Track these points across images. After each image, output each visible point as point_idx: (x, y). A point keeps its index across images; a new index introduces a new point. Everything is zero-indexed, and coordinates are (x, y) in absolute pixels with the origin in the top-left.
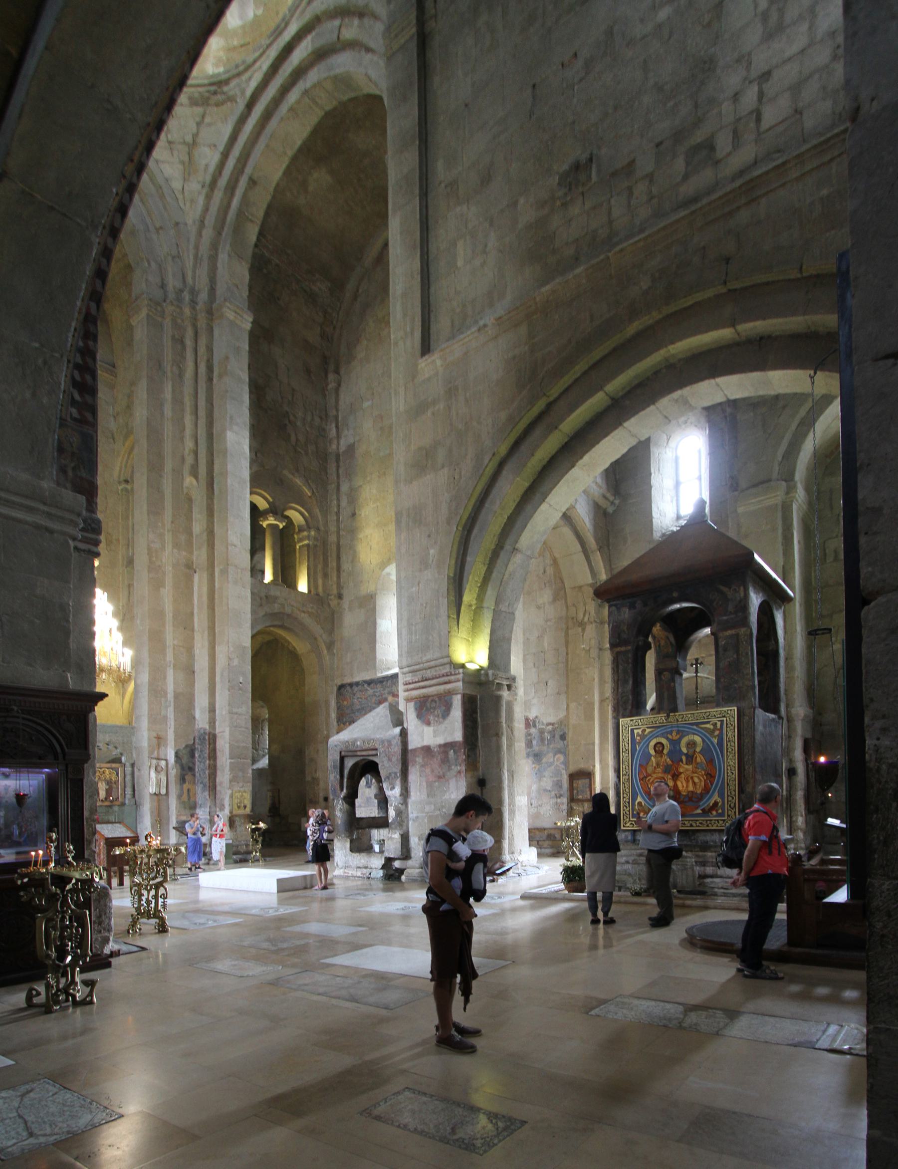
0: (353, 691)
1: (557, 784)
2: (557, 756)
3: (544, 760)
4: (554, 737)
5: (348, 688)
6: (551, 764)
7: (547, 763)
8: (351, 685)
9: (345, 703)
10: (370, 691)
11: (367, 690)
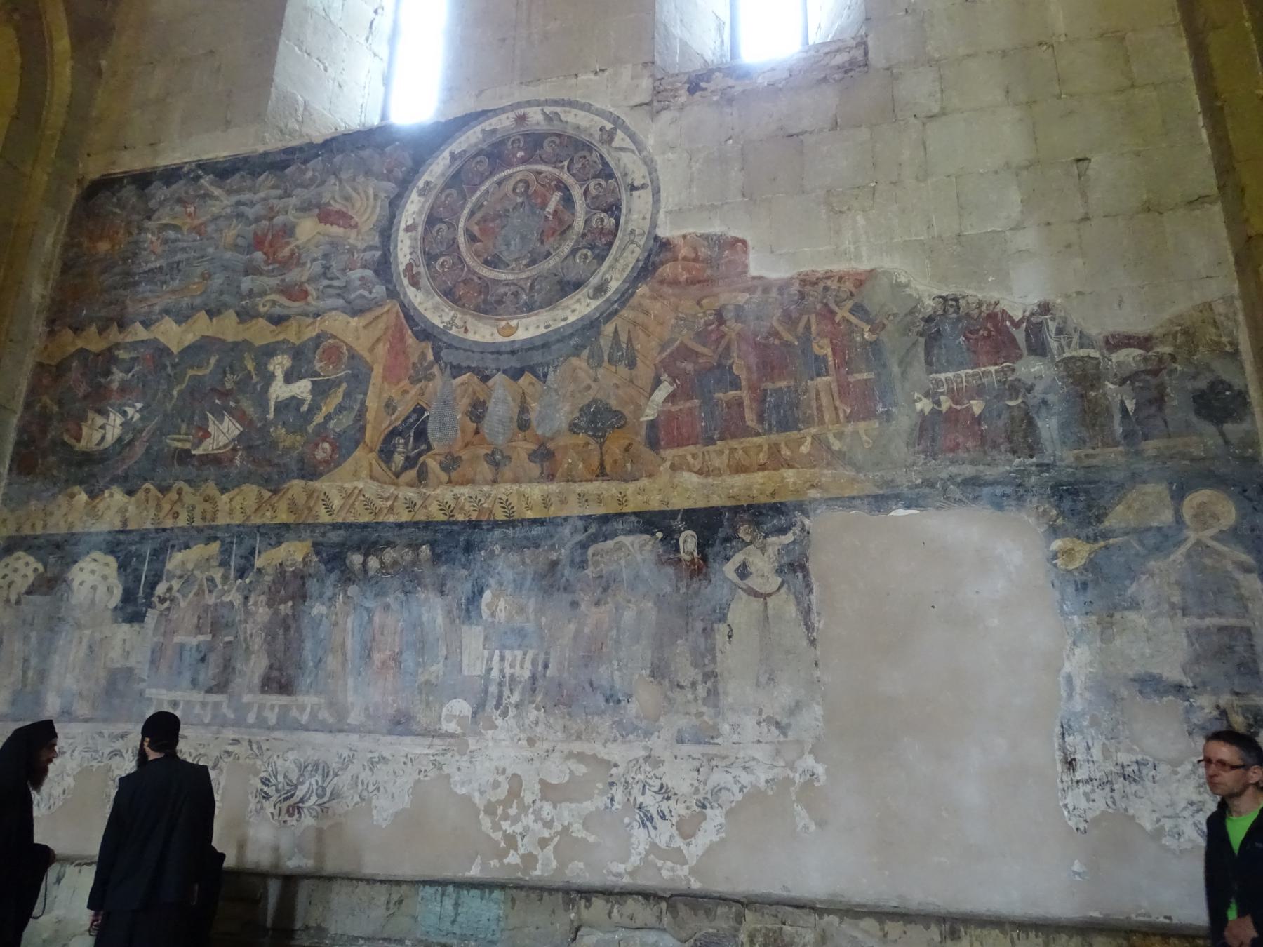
0: (144, 198)
1: (1224, 652)
2: (1203, 495)
3: (1118, 518)
4: (1159, 400)
5: (129, 192)
6: (1165, 540)
7: (1139, 532)
8: (143, 180)
9: (104, 246)
10: (222, 201)
11: (207, 195)
